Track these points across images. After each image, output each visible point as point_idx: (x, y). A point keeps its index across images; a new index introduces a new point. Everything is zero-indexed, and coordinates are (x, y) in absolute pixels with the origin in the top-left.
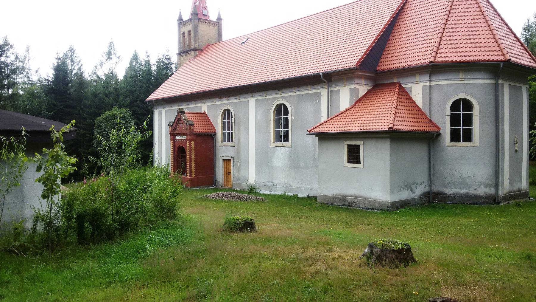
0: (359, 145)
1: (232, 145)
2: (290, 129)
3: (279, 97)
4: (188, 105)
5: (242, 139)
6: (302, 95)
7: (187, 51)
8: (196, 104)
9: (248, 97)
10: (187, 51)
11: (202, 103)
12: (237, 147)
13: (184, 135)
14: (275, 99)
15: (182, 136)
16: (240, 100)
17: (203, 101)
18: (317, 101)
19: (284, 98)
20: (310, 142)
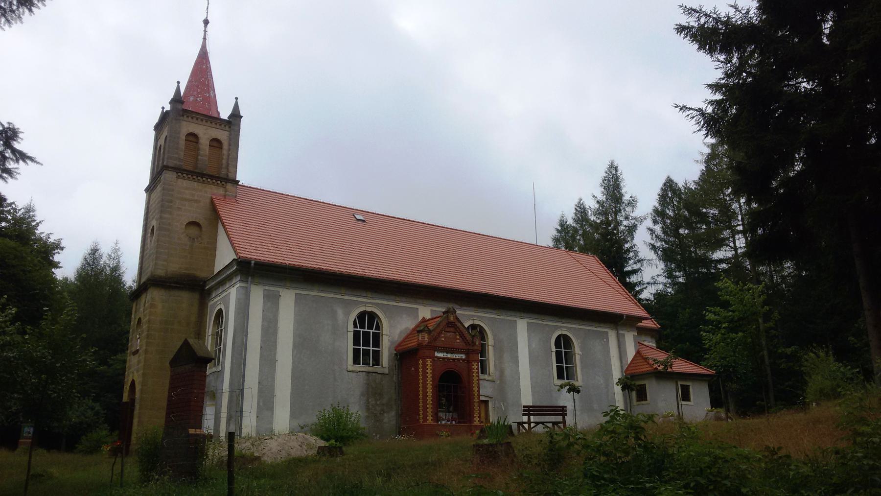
0: (689, 386)
1: (490, 378)
2: (555, 365)
3: (561, 327)
4: (379, 299)
5: (508, 372)
6: (589, 330)
7: (211, 177)
8: (401, 302)
9: (515, 316)
10: (211, 177)
11: (416, 303)
12: (498, 382)
13: (461, 353)
14: (556, 328)
15: (453, 353)
16: (501, 317)
17: (420, 301)
18: (605, 340)
19: (569, 329)
20: (602, 382)
